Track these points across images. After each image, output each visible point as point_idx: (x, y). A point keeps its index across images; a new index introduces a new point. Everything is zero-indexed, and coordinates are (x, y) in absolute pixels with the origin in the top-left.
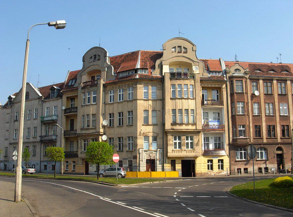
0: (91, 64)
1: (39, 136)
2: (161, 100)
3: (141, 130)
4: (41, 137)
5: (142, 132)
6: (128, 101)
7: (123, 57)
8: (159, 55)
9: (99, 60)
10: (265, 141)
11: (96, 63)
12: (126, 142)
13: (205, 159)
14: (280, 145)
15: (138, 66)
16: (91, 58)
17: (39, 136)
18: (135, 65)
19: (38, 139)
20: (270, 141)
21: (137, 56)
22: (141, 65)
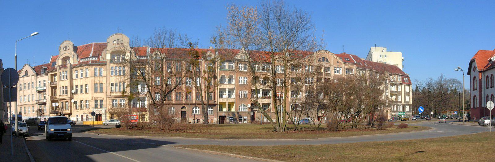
0: (64, 52)
1: (36, 100)
2: (105, 77)
3: (93, 96)
4: (37, 101)
5: (94, 97)
6: (85, 78)
7: (84, 47)
8: (104, 46)
9: (69, 49)
10: (174, 102)
11: (68, 51)
12: (84, 104)
13: (75, 105)
14: (184, 106)
15: (91, 55)
16: (64, 48)
17: (36, 100)
18: (89, 54)
19: (35, 102)
20: (177, 102)
21: (92, 47)
22: (93, 54)
